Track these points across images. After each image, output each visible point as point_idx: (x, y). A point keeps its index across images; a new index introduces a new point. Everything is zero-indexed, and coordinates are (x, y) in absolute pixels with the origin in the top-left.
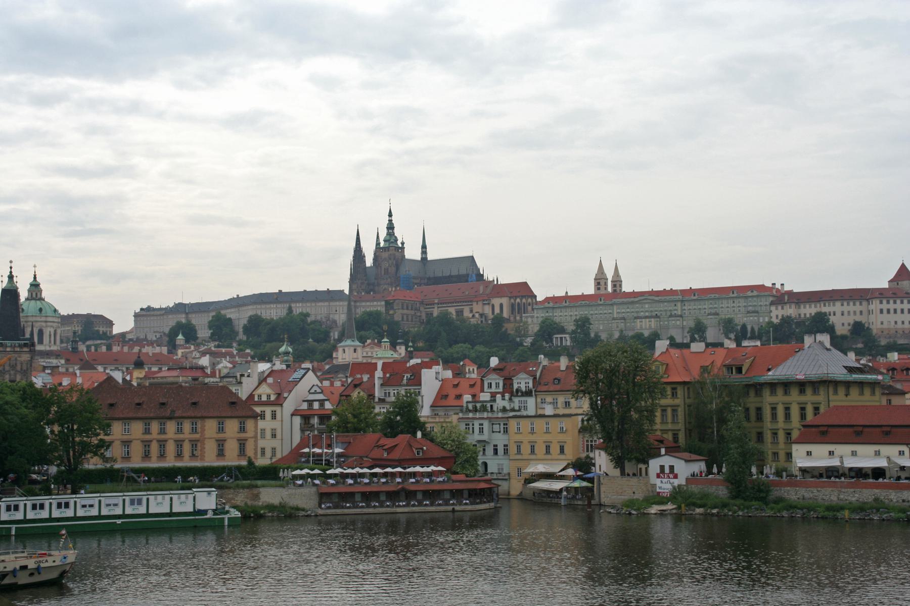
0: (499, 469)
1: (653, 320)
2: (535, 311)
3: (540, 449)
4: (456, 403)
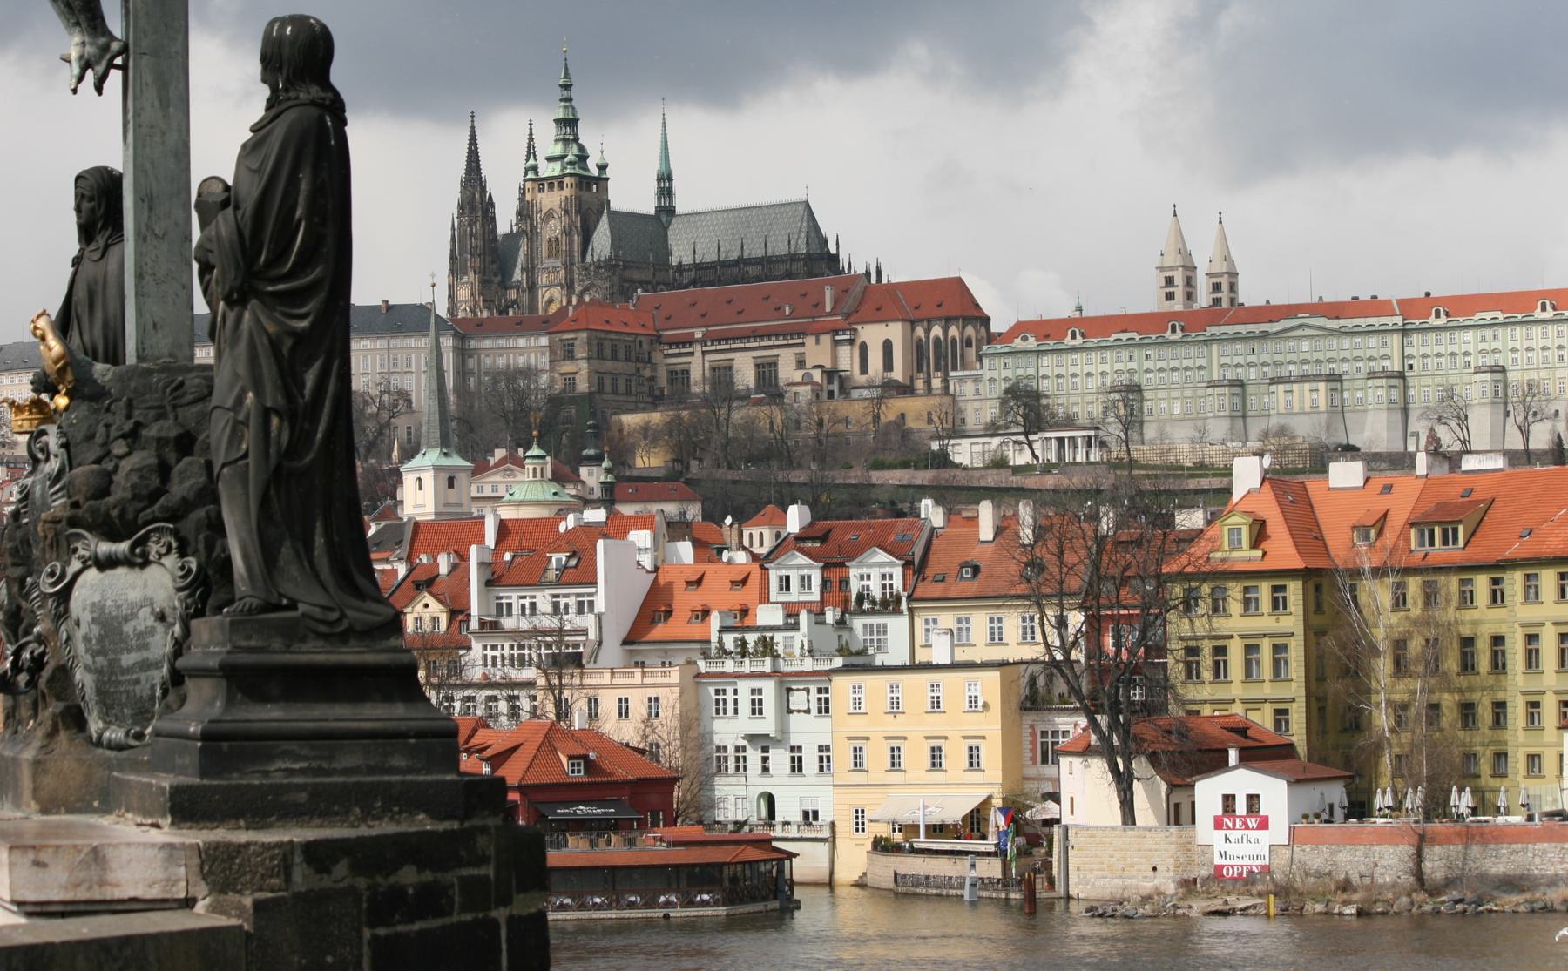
1: (1322, 386)
2: (986, 361)
3: (916, 756)
4: (695, 631)
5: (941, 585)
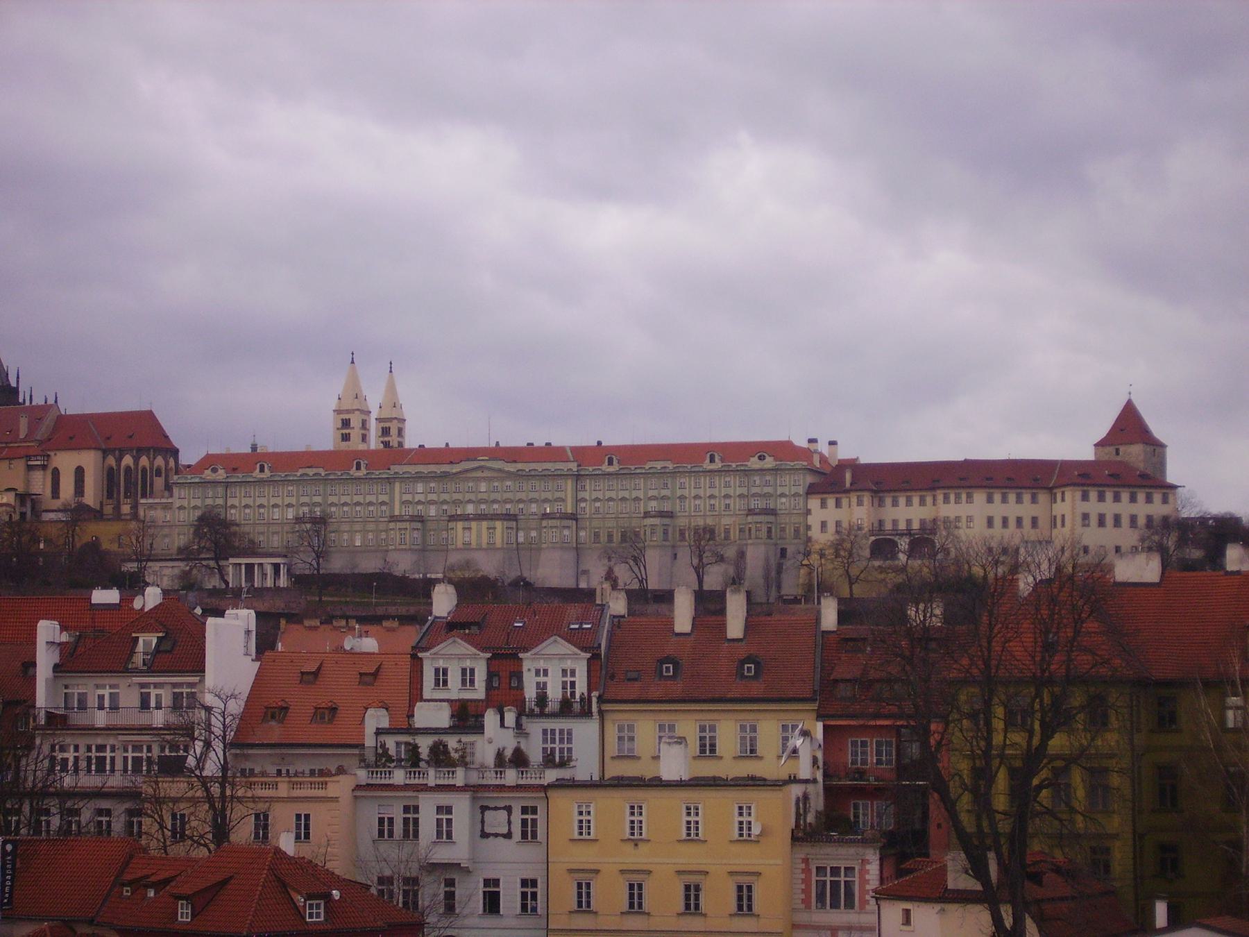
1: (498, 524)
2: (176, 490)
5: (637, 684)
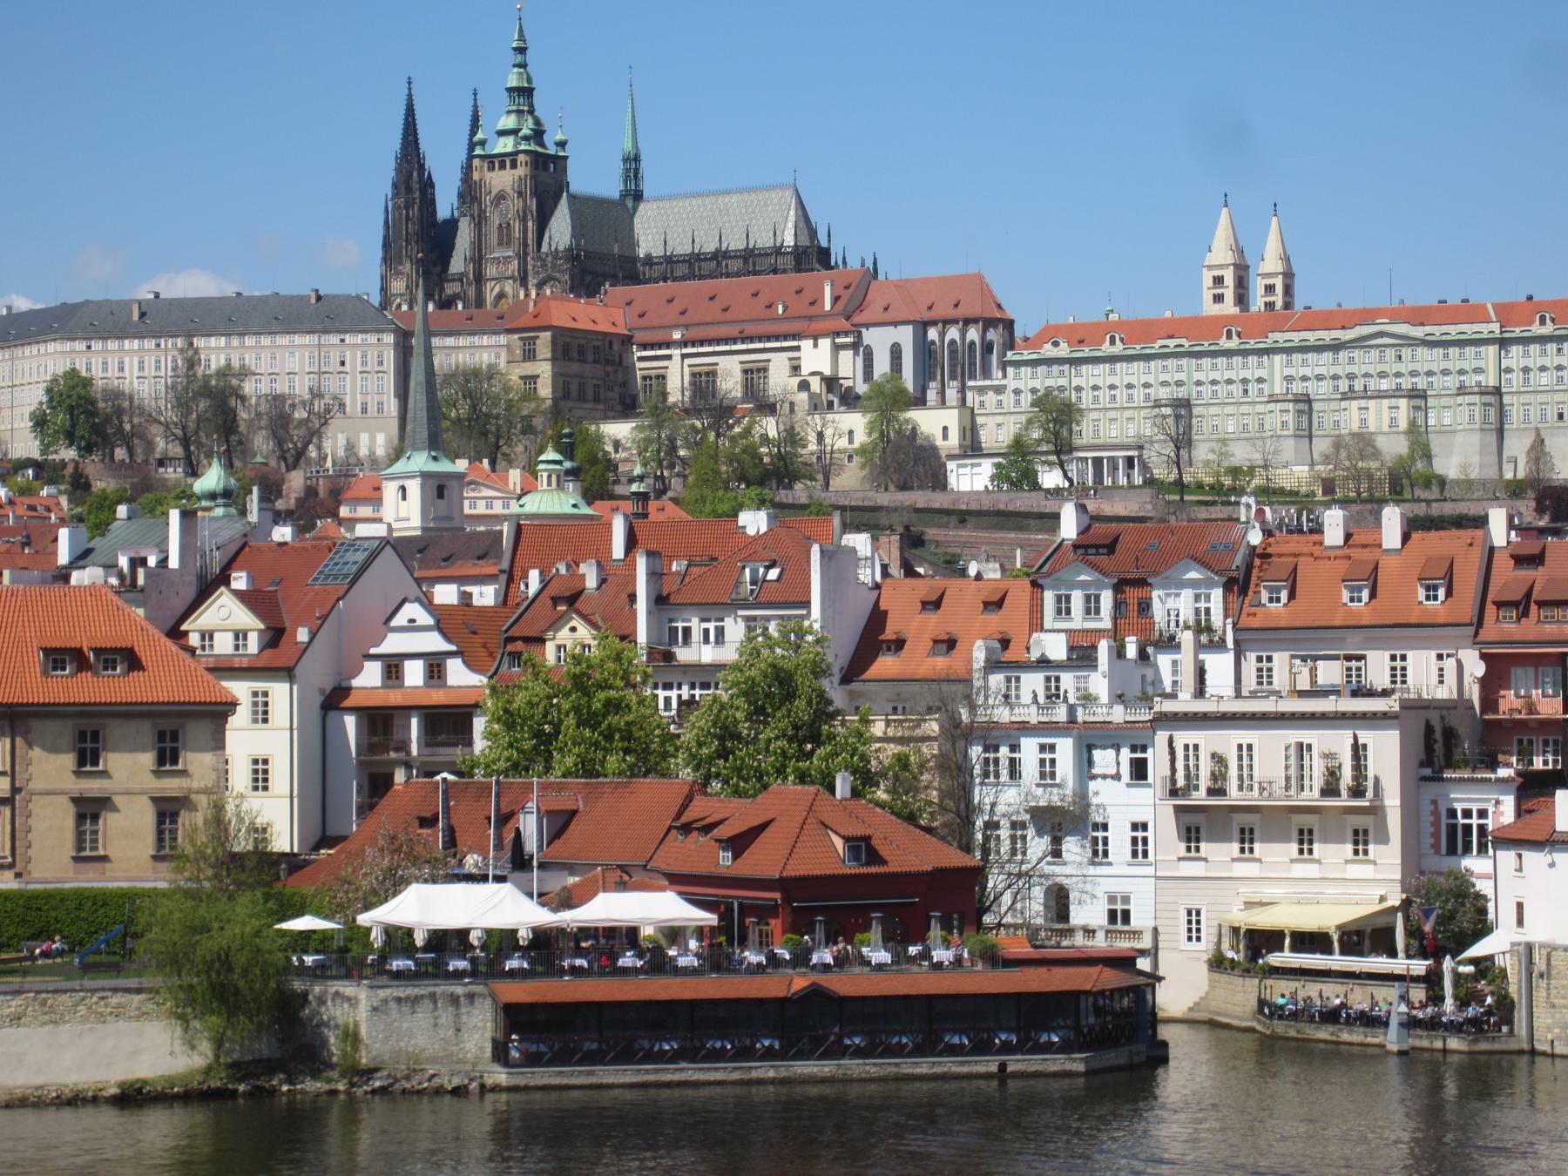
0: (1112, 915)
1: (1403, 403)
2: (1010, 370)
